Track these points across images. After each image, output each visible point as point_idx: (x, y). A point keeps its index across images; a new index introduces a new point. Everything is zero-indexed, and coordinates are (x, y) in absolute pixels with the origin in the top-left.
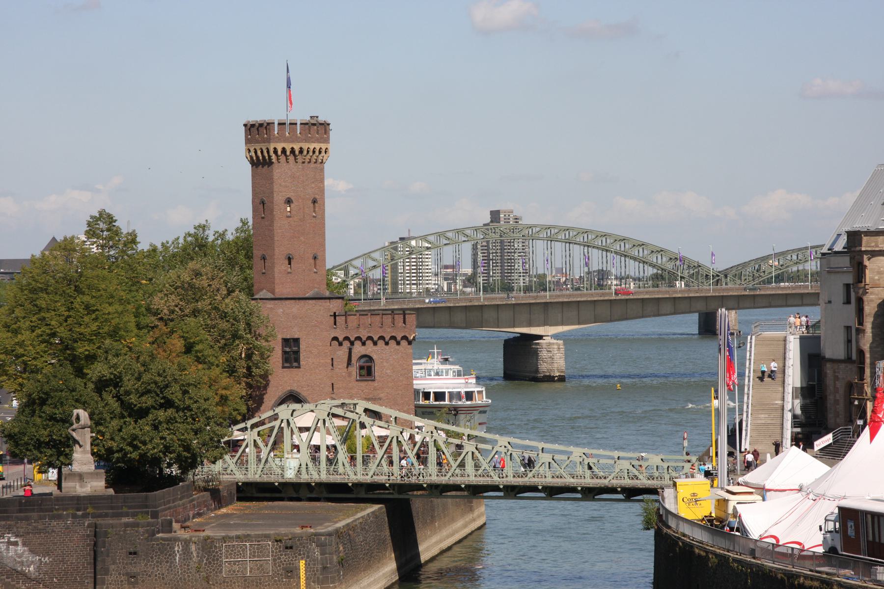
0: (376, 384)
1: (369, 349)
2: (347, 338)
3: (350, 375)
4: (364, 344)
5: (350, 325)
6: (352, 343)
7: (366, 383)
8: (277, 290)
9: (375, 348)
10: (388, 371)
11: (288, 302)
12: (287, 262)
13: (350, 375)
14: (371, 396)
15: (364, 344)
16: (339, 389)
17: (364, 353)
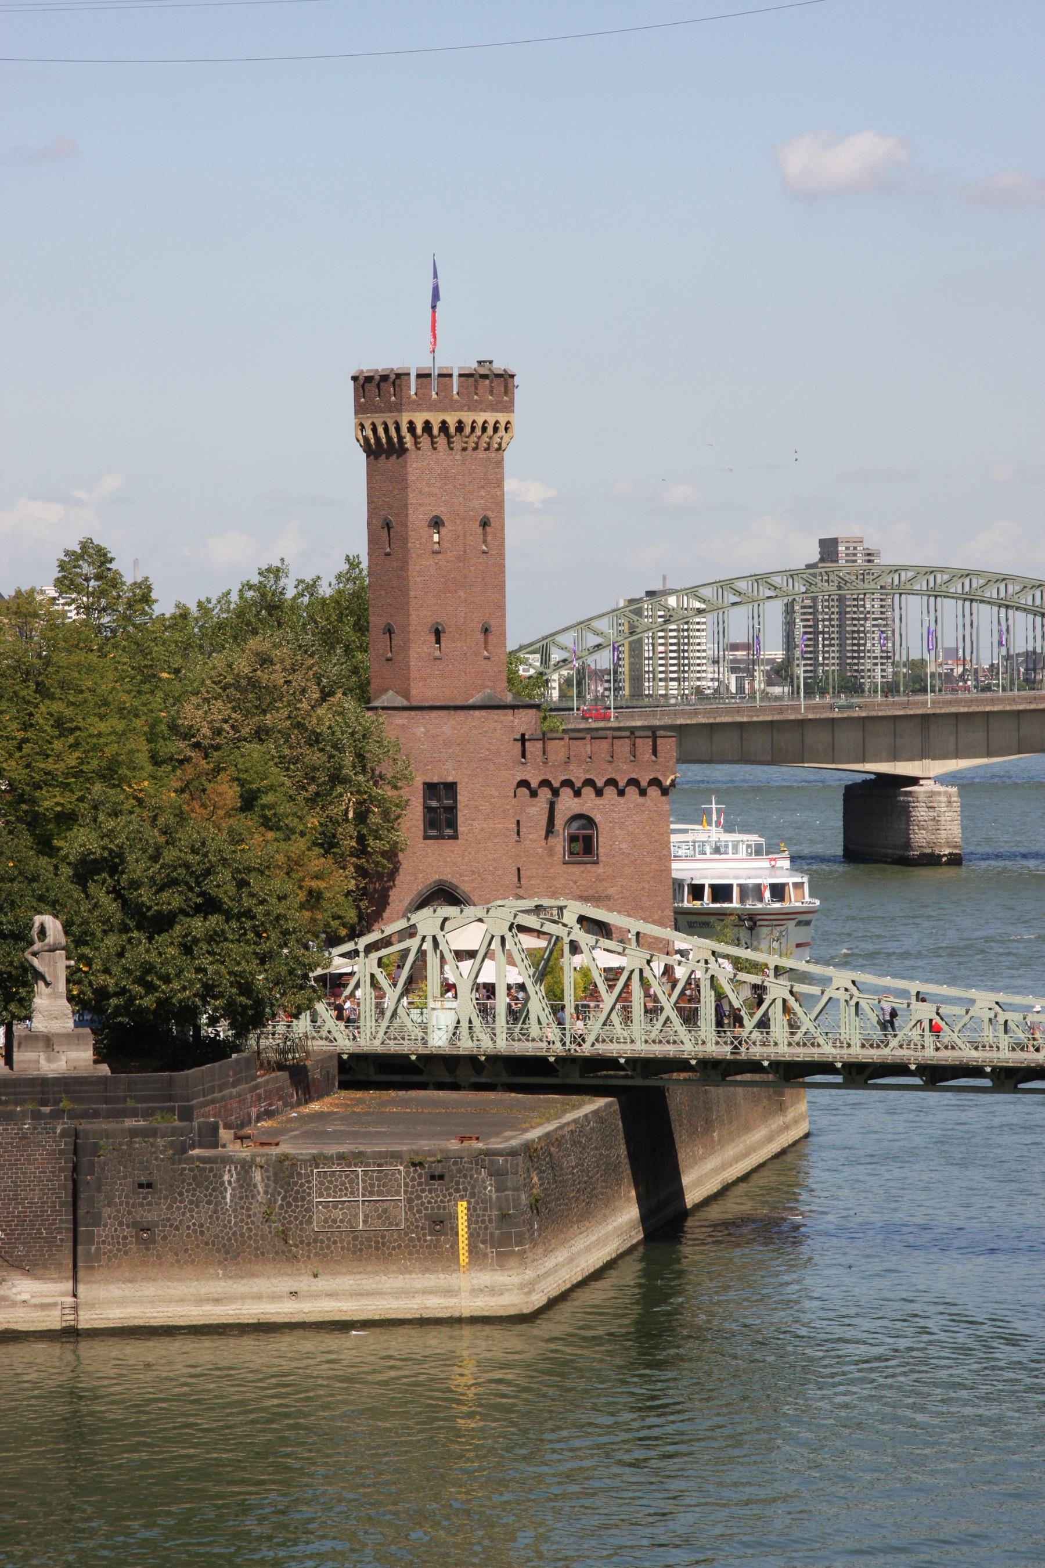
0: (600, 869)
1: (588, 803)
2: (545, 783)
3: (551, 851)
4: (577, 793)
5: (551, 757)
6: (556, 792)
7: (582, 867)
8: (413, 692)
9: (599, 801)
10: (624, 846)
11: (434, 714)
12: (433, 638)
13: (551, 851)
14: (591, 892)
15: (577, 793)
16: (530, 878)
17: (577, 811)
